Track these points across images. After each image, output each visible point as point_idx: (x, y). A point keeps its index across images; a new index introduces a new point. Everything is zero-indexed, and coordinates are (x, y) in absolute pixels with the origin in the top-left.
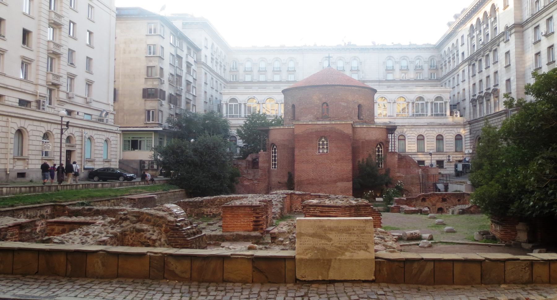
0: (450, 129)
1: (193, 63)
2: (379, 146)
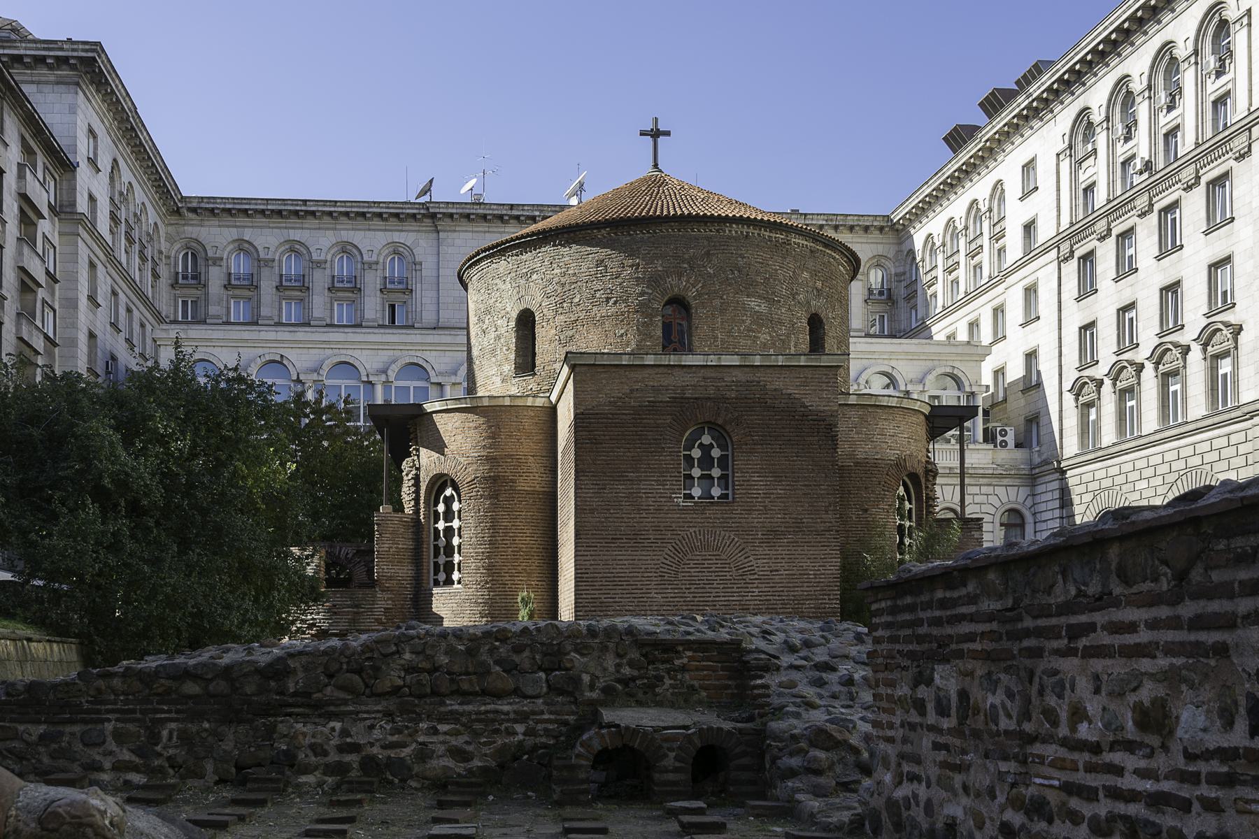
0: (984, 490)
1: (45, 211)
2: (901, 491)
